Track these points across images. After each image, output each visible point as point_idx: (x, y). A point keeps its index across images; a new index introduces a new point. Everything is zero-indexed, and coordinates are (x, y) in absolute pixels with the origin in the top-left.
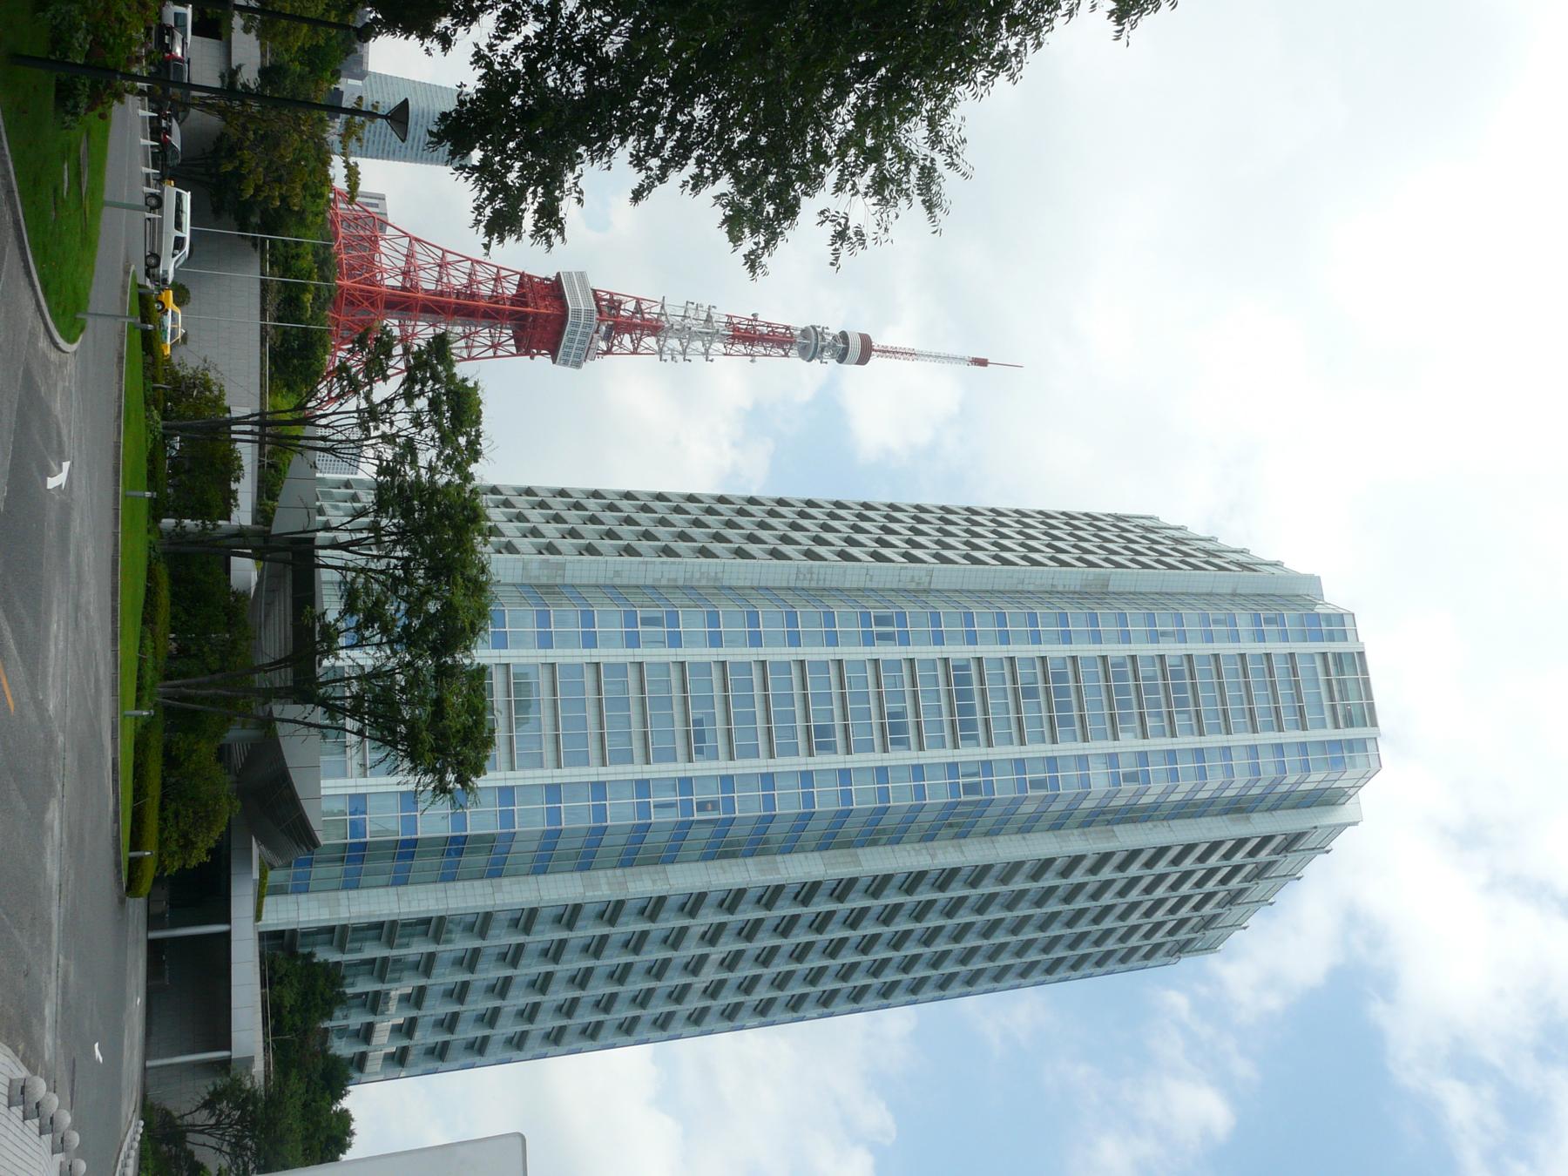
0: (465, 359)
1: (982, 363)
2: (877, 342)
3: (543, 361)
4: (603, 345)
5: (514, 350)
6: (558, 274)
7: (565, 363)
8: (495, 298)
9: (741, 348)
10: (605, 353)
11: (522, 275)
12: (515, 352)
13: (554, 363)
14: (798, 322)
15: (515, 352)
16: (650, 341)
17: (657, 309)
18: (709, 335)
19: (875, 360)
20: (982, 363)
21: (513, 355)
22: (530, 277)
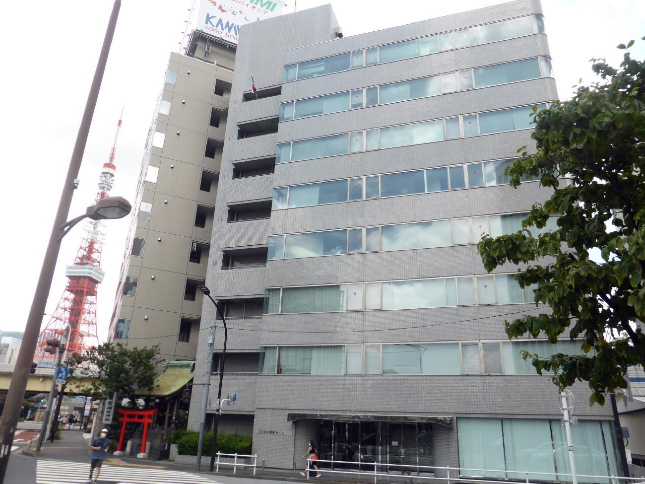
0: (96, 316)
1: (120, 122)
2: (108, 161)
4: (96, 264)
5: (94, 297)
6: (67, 276)
7: (102, 280)
13: (100, 283)
16: (96, 246)
19: (114, 163)
20: (120, 122)
21: (96, 298)
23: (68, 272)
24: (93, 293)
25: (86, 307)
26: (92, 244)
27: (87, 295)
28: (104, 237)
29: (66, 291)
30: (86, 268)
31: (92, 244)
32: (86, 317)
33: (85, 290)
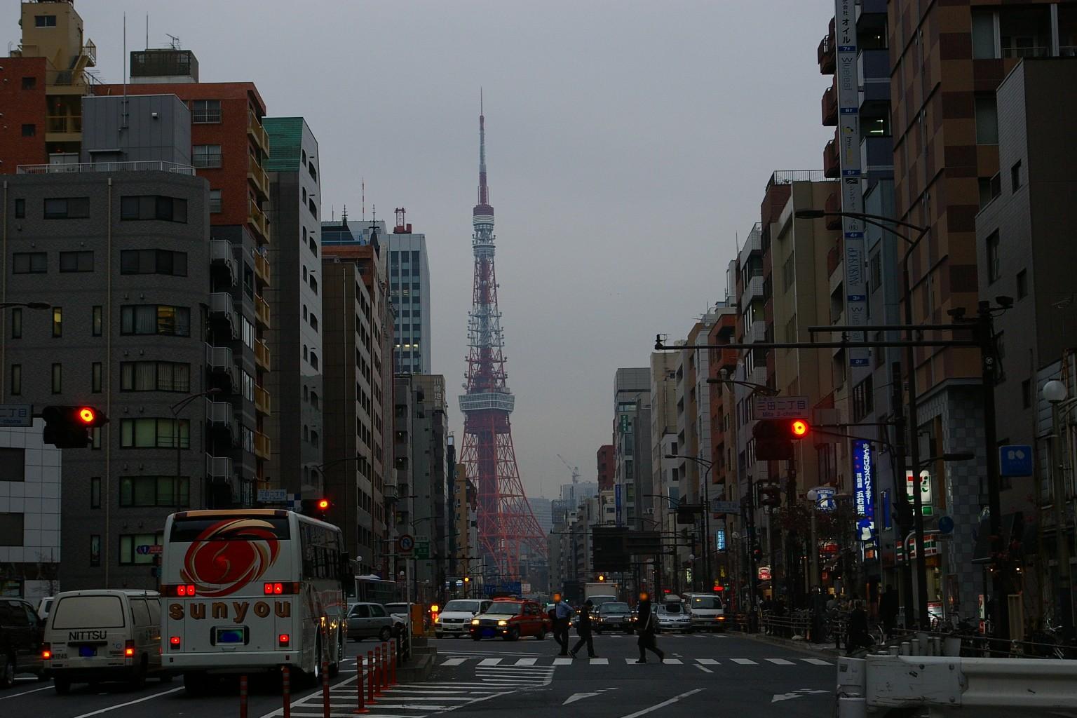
0: (515, 464)
1: (482, 119)
3: (512, 418)
7: (513, 405)
8: (480, 448)
9: (492, 291)
10: (504, 381)
11: (465, 432)
12: (508, 435)
14: (471, 259)
15: (508, 435)
17: (475, 348)
18: (484, 317)
20: (482, 119)
21: (510, 436)
22: (466, 428)
23: (466, 406)
24: (506, 429)
25: (500, 455)
26: (486, 351)
27: (496, 433)
28: (501, 333)
29: (467, 434)
30: (486, 397)
31: (486, 351)
32: (501, 469)
33: (493, 431)
